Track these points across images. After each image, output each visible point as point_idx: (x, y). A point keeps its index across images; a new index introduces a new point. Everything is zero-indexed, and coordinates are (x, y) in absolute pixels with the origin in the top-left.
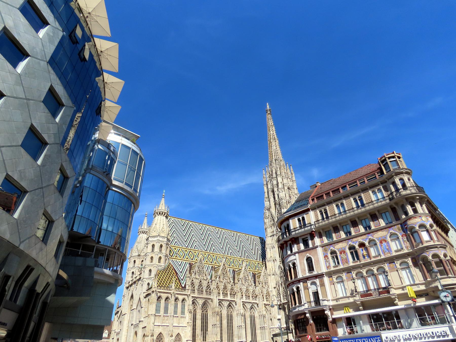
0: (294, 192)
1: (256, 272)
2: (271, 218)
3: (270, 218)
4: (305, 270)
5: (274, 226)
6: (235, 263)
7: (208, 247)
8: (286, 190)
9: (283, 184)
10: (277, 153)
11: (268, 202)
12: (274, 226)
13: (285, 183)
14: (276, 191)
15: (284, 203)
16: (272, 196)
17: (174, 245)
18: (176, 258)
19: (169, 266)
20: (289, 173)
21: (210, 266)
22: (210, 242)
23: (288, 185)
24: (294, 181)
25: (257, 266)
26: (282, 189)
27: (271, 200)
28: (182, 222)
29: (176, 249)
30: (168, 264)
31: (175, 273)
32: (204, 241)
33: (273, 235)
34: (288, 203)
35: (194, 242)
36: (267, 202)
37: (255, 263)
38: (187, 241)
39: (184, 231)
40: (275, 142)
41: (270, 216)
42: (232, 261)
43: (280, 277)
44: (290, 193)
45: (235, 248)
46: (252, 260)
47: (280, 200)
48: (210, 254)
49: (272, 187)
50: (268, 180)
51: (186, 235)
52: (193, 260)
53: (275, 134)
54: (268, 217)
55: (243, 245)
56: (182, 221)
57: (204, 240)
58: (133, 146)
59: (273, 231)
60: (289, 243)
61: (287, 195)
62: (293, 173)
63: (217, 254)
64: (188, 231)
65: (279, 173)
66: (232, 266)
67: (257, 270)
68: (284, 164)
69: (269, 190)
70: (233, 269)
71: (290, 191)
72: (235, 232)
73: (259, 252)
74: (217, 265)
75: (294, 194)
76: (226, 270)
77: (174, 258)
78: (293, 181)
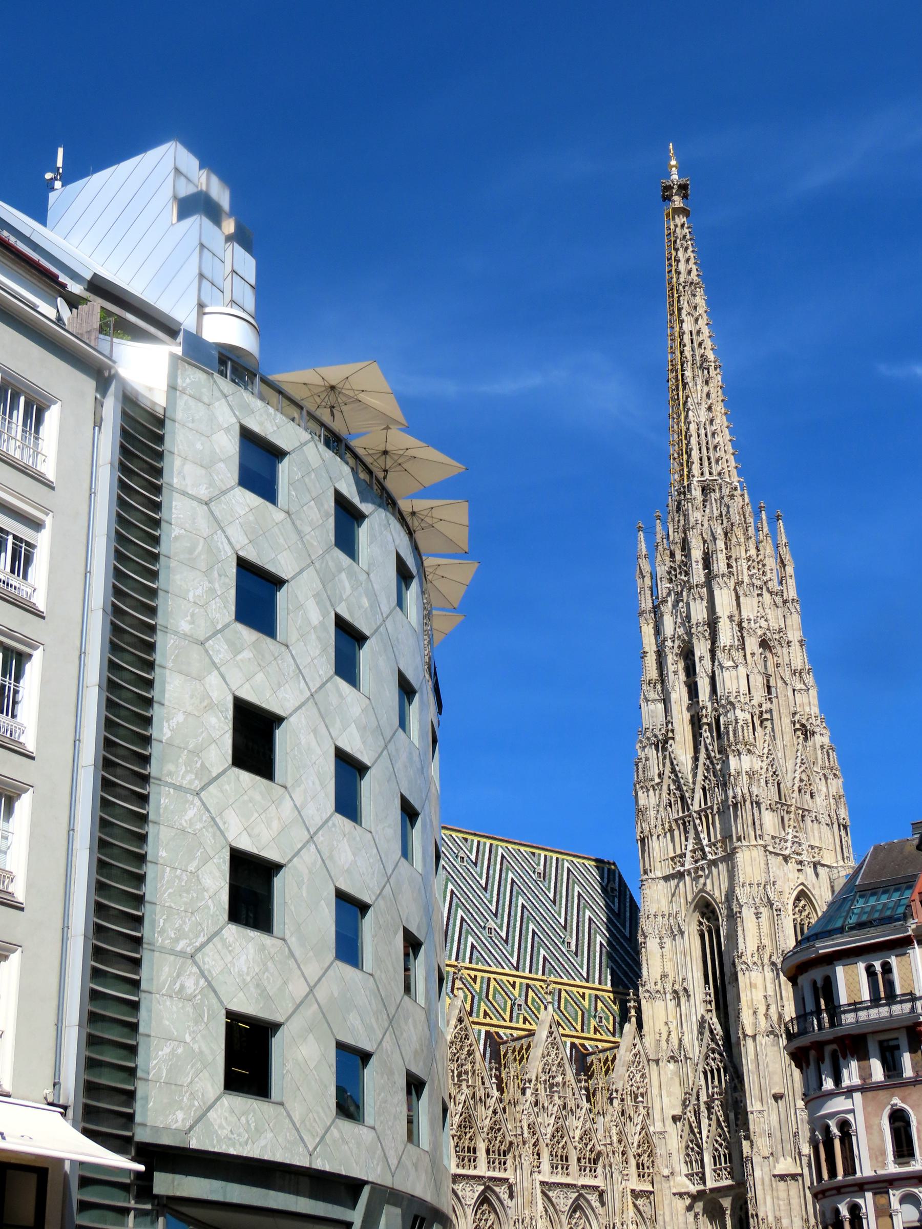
0: (789, 665)
1: (587, 1043)
2: (672, 787)
3: (665, 787)
4: (883, 1153)
5: (686, 832)
8: (753, 654)
9: (740, 625)
10: (715, 447)
11: (660, 706)
12: (686, 832)
13: (749, 620)
14: (701, 658)
15: (741, 723)
16: (682, 676)
20: (771, 563)
23: (764, 624)
24: (789, 605)
25: (589, 1011)
26: (733, 652)
27: (674, 696)
33: (680, 875)
34: (757, 723)
36: (652, 706)
37: (583, 997)
40: (707, 383)
41: (666, 781)
42: (481, 987)
43: (705, 1073)
44: (771, 670)
45: (491, 924)
46: (565, 980)
47: (724, 706)
49: (681, 631)
50: (665, 592)
53: (706, 331)
54: (657, 780)
55: (523, 906)
59: (678, 852)
60: (828, 1049)
61: (758, 681)
62: (788, 558)
65: (720, 565)
66: (482, 1014)
67: (592, 1030)
68: (748, 509)
69: (669, 643)
70: (488, 1028)
71: (769, 656)
72: (482, 840)
73: (599, 938)
75: (787, 675)
76: (471, 1045)
78: (785, 602)
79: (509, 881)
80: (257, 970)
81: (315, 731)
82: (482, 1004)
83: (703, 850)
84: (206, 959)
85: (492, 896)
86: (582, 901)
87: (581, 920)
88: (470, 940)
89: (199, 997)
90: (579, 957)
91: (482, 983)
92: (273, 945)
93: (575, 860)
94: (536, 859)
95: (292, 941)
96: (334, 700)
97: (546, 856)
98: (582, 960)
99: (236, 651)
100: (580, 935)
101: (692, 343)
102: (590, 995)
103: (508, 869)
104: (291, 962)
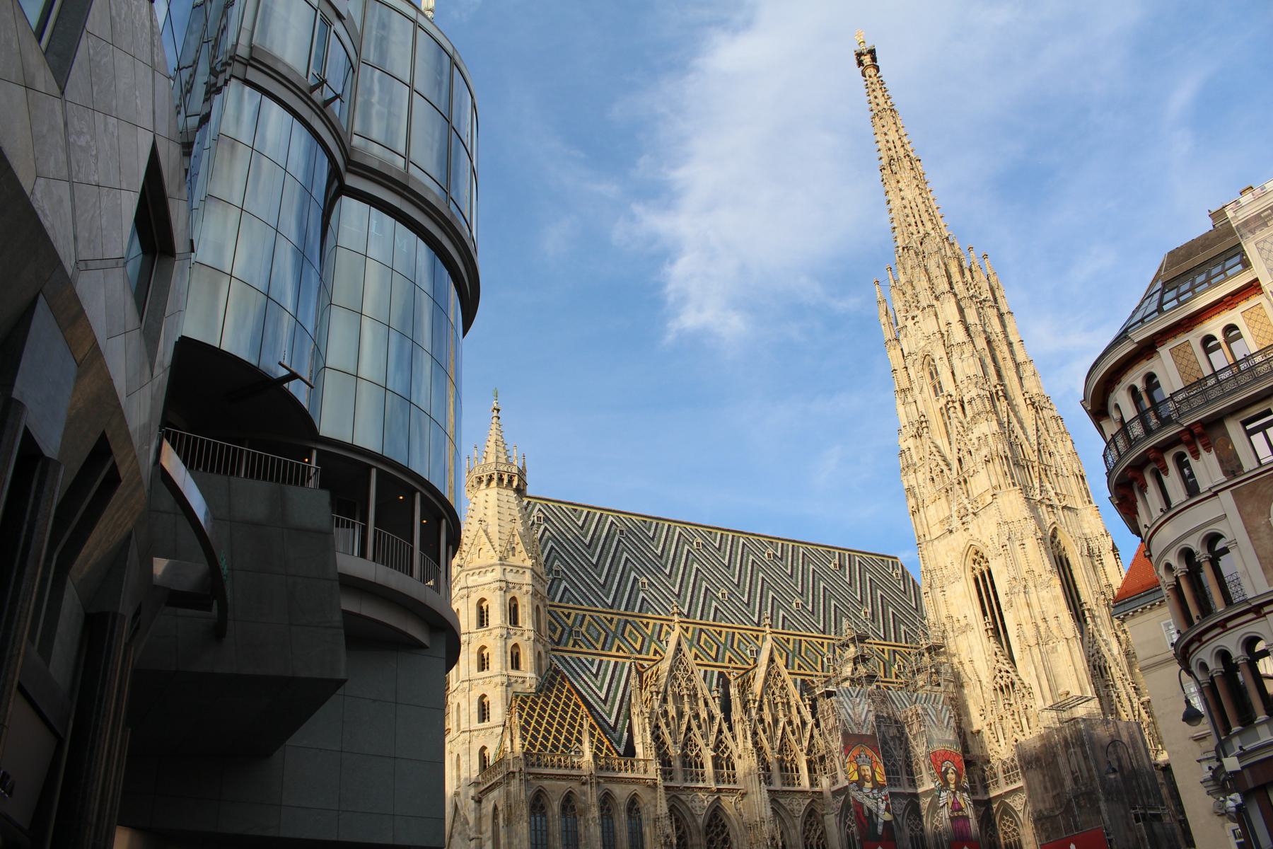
6: (806, 654)
7: (694, 601)
17: (560, 601)
18: (577, 648)
19: (556, 680)
21: (713, 672)
22: (697, 585)
25: (889, 661)
28: (577, 514)
29: (572, 617)
30: (551, 673)
31: (580, 703)
32: (675, 581)
35: (636, 587)
38: (609, 583)
39: (589, 546)
42: (794, 647)
48: (704, 627)
51: (601, 562)
52: (644, 652)
56: (575, 510)
57: (673, 576)
58: (420, 15)
63: (731, 625)
64: (607, 546)
66: (796, 667)
67: (894, 676)
70: (803, 677)
72: (785, 543)
74: (739, 665)
77: (570, 648)
79: (811, 570)
82: (796, 659)
85: (797, 582)
86: (873, 584)
87: (874, 597)
88: (781, 612)
90: (876, 624)
91: (794, 643)
94: (831, 555)
97: (839, 553)
98: (879, 626)
100: (875, 607)
101: (895, 147)
102: (889, 650)
103: (809, 563)
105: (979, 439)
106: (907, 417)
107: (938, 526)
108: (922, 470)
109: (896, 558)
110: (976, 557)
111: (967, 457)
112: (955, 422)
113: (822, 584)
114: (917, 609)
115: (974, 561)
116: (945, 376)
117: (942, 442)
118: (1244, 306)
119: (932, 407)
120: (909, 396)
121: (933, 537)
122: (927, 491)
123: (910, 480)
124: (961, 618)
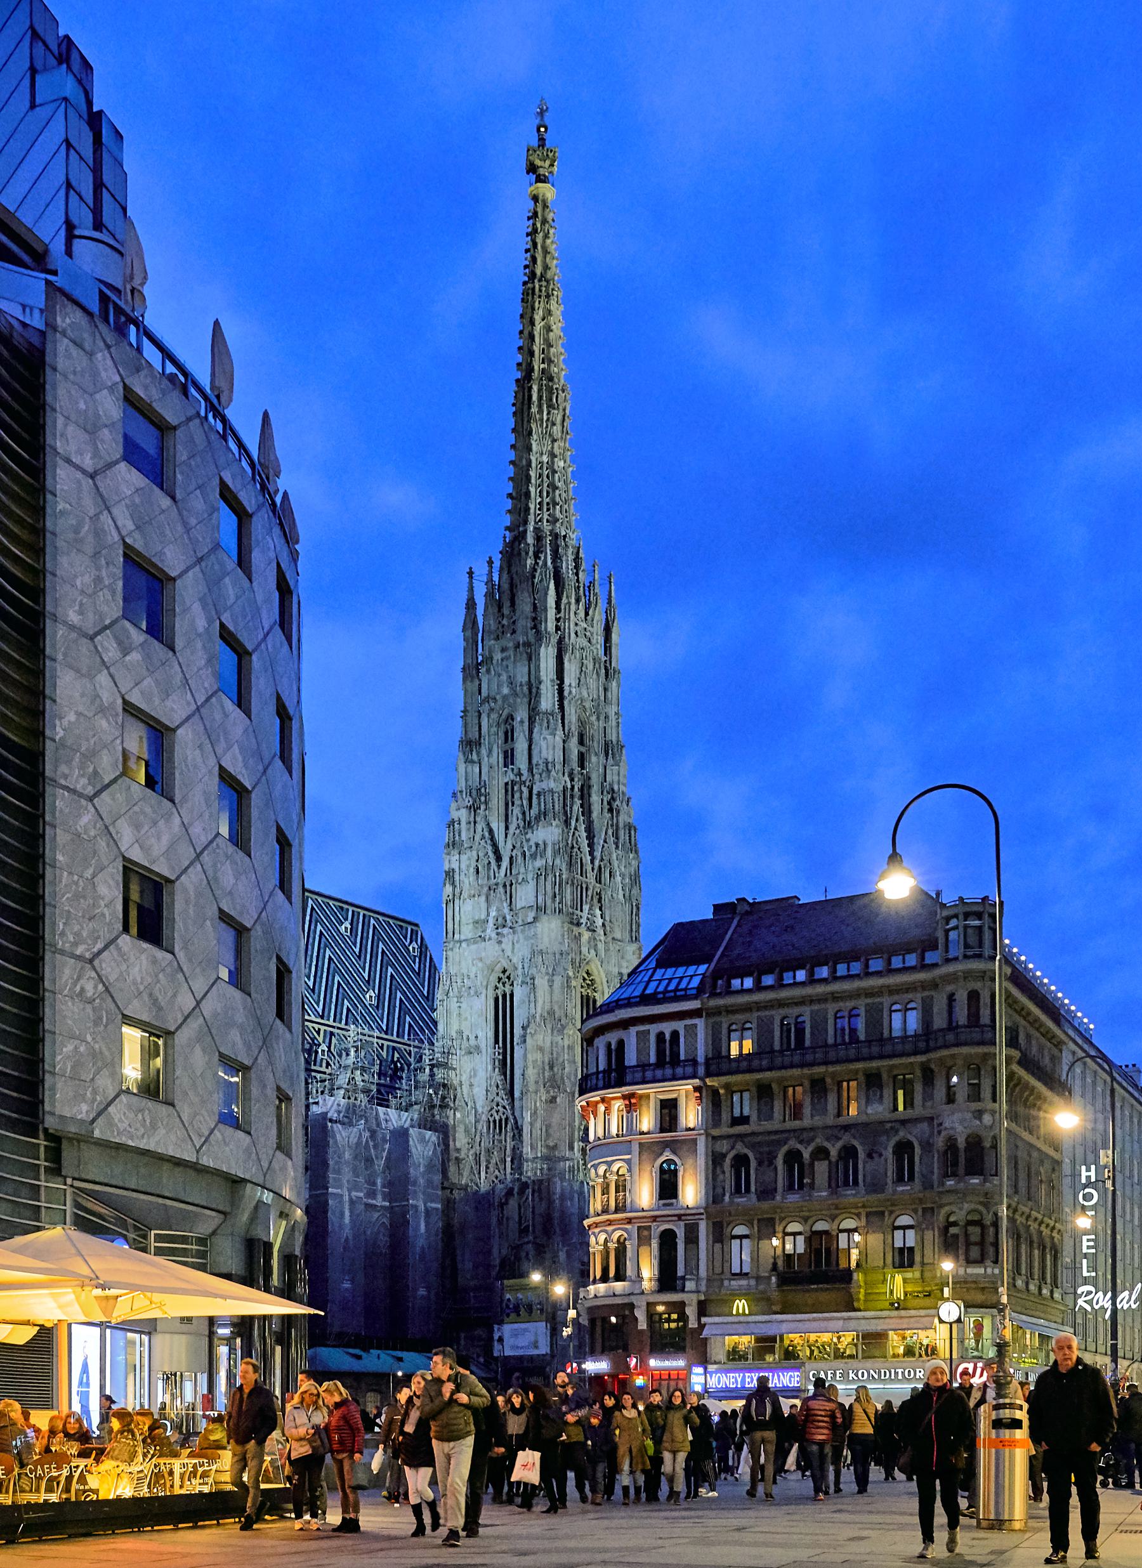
59: (483, 917)
79: (318, 933)
80: (150, 980)
81: (200, 747)
83: (504, 918)
84: (104, 965)
86: (385, 958)
89: (97, 1001)
92: (164, 958)
93: (381, 918)
95: (180, 954)
96: (218, 716)
99: (125, 651)
103: (317, 921)
104: (180, 976)
105: (537, 845)
106: (466, 780)
107: (471, 926)
108: (468, 852)
109: (416, 925)
110: (501, 975)
111: (520, 859)
112: (517, 811)
113: (328, 952)
114: (427, 998)
115: (500, 979)
116: (521, 745)
117: (498, 826)
118: (689, 1022)
119: (498, 780)
120: (474, 753)
121: (463, 938)
122: (467, 881)
123: (452, 861)
124: (472, 1038)
